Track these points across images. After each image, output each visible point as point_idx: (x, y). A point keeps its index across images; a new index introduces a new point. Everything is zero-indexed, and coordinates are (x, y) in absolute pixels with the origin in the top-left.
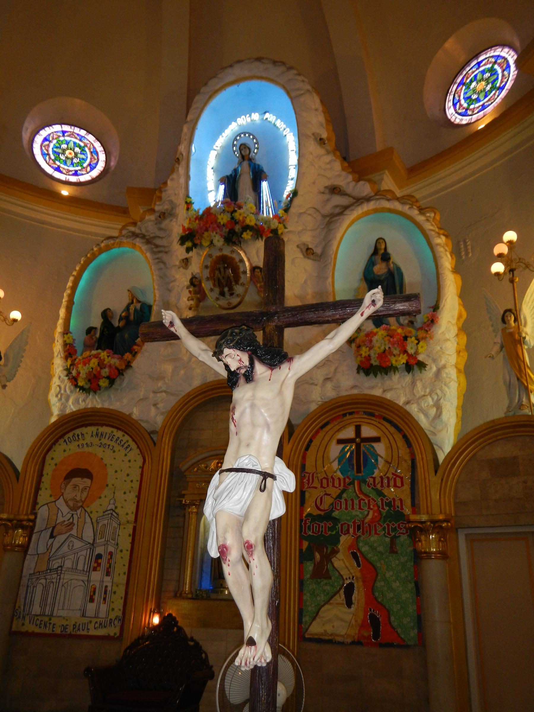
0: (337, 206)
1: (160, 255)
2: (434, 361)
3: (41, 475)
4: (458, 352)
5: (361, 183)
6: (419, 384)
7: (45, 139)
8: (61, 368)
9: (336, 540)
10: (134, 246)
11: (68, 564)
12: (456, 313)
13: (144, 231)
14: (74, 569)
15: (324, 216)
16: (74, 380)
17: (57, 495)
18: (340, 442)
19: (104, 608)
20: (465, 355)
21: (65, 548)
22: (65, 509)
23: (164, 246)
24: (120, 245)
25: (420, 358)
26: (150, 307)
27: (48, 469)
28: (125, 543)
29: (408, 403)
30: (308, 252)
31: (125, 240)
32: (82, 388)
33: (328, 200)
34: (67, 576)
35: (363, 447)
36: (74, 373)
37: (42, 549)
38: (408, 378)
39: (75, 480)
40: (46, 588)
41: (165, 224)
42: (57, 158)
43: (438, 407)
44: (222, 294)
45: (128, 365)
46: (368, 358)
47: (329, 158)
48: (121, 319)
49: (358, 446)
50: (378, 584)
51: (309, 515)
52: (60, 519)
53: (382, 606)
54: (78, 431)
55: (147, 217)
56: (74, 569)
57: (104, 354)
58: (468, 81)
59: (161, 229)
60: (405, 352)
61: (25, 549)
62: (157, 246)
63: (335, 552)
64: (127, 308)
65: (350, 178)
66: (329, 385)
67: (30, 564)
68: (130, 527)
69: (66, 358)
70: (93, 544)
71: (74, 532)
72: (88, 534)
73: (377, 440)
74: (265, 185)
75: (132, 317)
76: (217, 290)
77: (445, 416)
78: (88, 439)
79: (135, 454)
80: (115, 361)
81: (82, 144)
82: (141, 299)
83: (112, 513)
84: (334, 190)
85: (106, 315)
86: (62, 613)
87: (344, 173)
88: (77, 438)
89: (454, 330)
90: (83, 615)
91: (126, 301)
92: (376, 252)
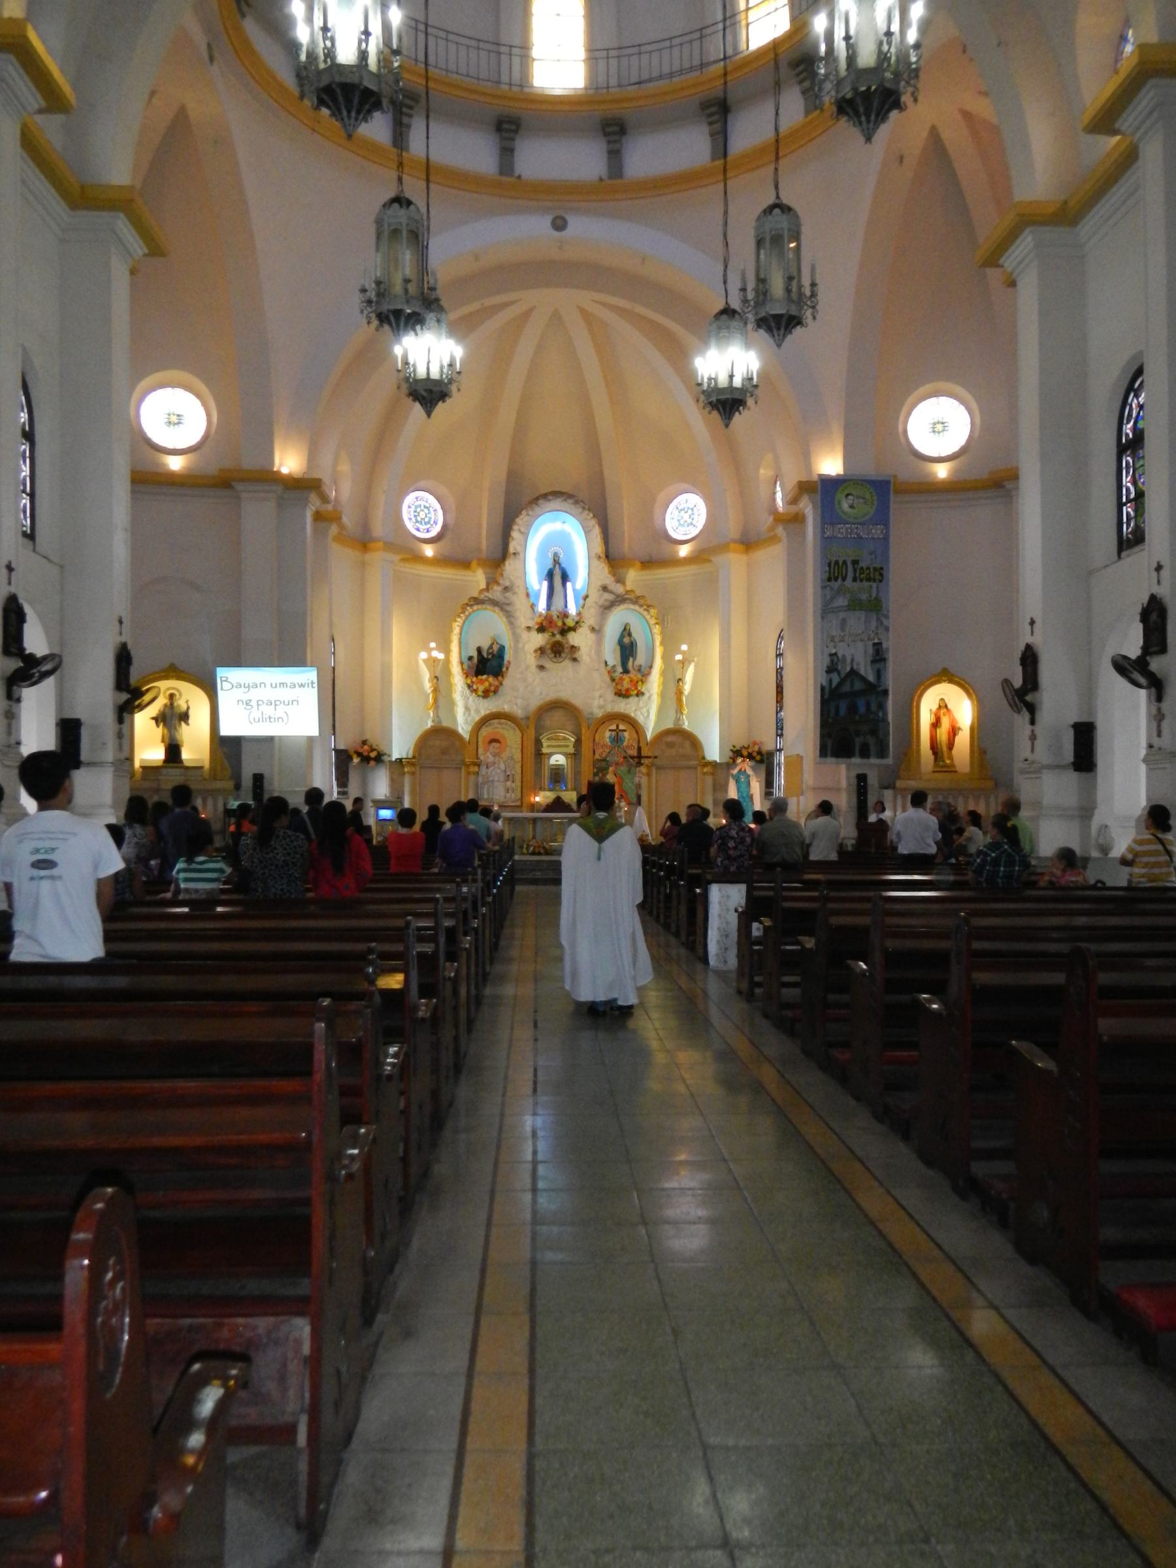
0: (606, 600)
1: (511, 619)
2: (649, 692)
3: (477, 742)
4: (659, 686)
5: (618, 584)
6: (641, 702)
7: (409, 507)
8: (462, 682)
9: (607, 769)
10: (494, 611)
11: (496, 779)
12: (659, 668)
13: (495, 598)
14: (498, 781)
15: (601, 606)
16: (475, 691)
17: (486, 751)
18: (610, 730)
19: (513, 795)
20: (661, 687)
21: (493, 773)
22: (491, 757)
23: (510, 612)
24: (485, 609)
25: (643, 690)
26: (504, 647)
27: (480, 739)
28: (519, 770)
29: (636, 710)
30: (593, 629)
31: (488, 607)
32: (479, 696)
33: (601, 596)
34: (496, 784)
35: (620, 733)
36: (475, 687)
37: (484, 773)
38: (636, 699)
39: (494, 744)
40: (488, 789)
41: (507, 594)
42: (417, 522)
43: (649, 714)
44: (555, 657)
45: (501, 684)
46: (620, 690)
47: (603, 565)
48: (488, 654)
49: (617, 733)
50: (624, 784)
51: (597, 760)
52: (489, 761)
53: (625, 792)
54: (491, 722)
55: (496, 588)
56: (498, 781)
57: (491, 679)
58: (680, 508)
59: (505, 598)
60: (636, 688)
61: (478, 773)
62: (507, 612)
63: (608, 773)
64: (491, 647)
65: (613, 579)
66: (602, 700)
67: (480, 780)
68: (520, 765)
69: (467, 677)
70: (505, 771)
71: (496, 766)
72: (502, 766)
73: (625, 731)
74: (569, 585)
75: (495, 652)
76: (553, 655)
77: (650, 717)
78: (496, 725)
79: (518, 733)
80: (497, 683)
81: (427, 505)
82: (499, 642)
83: (512, 758)
84: (605, 588)
85: (479, 650)
86: (498, 797)
87: (609, 576)
88: (491, 725)
89: (658, 676)
90: (505, 797)
91: (490, 643)
92: (625, 629)
